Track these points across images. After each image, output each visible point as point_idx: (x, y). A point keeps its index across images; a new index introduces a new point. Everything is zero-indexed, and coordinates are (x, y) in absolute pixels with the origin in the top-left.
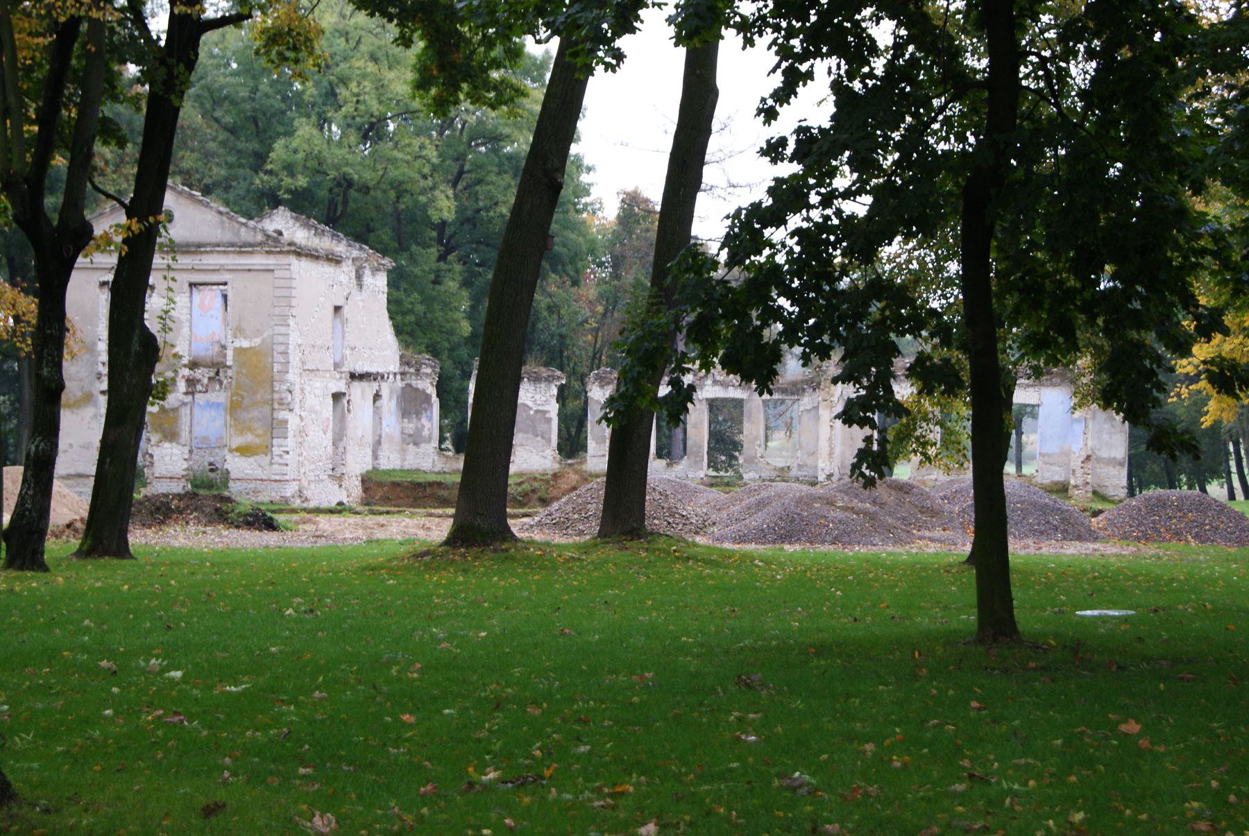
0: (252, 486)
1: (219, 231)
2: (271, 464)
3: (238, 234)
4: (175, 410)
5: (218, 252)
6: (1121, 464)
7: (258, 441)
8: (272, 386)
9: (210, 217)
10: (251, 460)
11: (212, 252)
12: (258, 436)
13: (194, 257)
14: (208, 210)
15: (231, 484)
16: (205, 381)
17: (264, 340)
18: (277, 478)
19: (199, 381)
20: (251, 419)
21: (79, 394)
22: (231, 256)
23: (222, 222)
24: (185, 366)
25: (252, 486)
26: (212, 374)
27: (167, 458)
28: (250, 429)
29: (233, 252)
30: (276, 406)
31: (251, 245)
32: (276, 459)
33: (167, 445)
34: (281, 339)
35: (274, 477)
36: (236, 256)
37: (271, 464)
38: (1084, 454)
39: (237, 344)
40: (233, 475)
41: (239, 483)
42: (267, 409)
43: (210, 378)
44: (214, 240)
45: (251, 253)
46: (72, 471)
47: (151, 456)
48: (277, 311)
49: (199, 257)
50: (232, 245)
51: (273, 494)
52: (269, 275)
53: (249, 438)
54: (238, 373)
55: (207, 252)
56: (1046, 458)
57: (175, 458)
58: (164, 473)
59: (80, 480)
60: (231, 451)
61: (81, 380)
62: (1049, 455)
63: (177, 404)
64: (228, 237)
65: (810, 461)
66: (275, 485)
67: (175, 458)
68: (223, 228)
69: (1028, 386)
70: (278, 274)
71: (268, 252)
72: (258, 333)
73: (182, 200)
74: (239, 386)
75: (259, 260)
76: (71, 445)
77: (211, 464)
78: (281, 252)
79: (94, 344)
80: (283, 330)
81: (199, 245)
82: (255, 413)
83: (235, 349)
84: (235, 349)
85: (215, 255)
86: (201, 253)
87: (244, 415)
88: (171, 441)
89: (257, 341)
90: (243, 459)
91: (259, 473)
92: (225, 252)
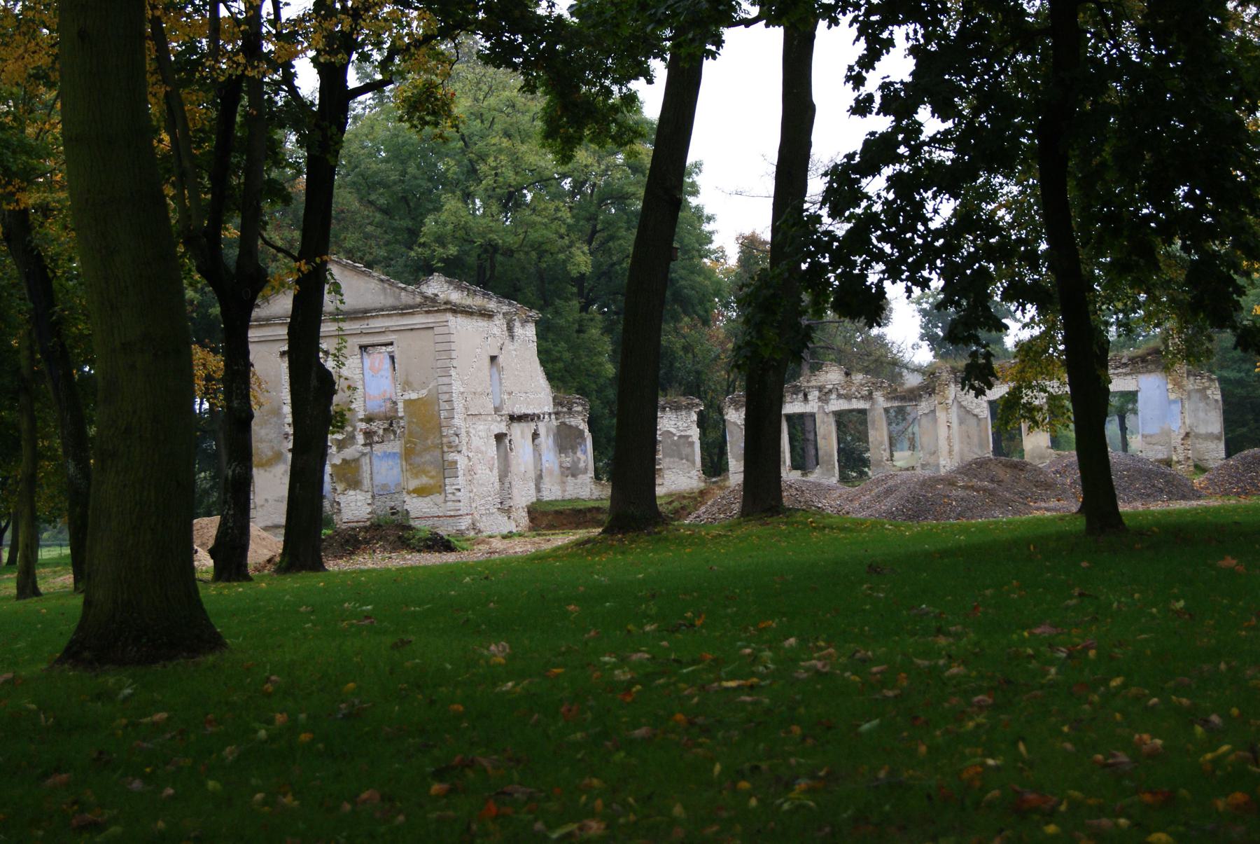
0: (430, 523)
2: (446, 501)
3: (399, 298)
4: (356, 460)
6: (1218, 438)
7: (432, 482)
8: (441, 432)
10: (428, 499)
11: (377, 316)
12: (432, 477)
16: (381, 432)
19: (375, 433)
20: (424, 463)
21: (270, 454)
23: (384, 289)
24: (361, 420)
25: (430, 523)
26: (386, 426)
28: (425, 473)
30: (446, 449)
31: (411, 307)
32: (450, 496)
33: (352, 492)
34: (445, 388)
38: (1183, 432)
39: (406, 397)
40: (412, 515)
42: (437, 453)
43: (384, 429)
44: (379, 306)
46: (269, 524)
47: (338, 503)
48: (439, 364)
50: (395, 308)
52: (430, 332)
53: (424, 480)
54: (409, 423)
56: (1149, 439)
60: (409, 493)
61: (271, 441)
62: (1151, 436)
63: (357, 455)
64: (390, 301)
65: (931, 460)
69: (1126, 374)
70: (437, 330)
71: (427, 312)
72: (424, 385)
73: (347, 273)
74: (411, 434)
75: (419, 320)
76: (266, 500)
77: (392, 508)
78: (437, 311)
79: (280, 408)
80: (446, 380)
81: (366, 311)
83: (406, 402)
84: (406, 402)
85: (380, 319)
86: (368, 318)
87: (418, 460)
89: (424, 393)
92: (388, 315)
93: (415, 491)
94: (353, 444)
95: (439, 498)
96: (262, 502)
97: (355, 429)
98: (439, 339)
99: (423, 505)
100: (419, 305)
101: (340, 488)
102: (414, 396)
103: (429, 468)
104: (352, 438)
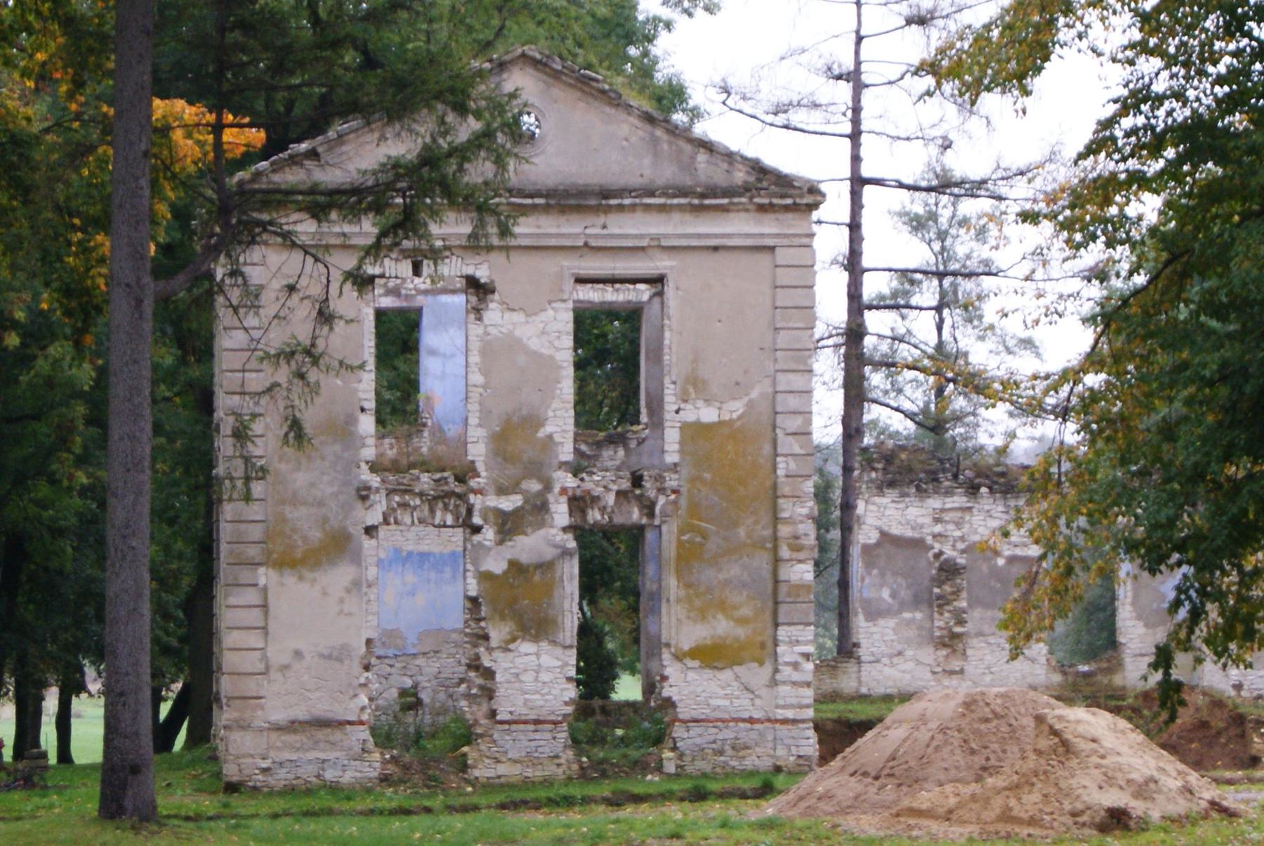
0: (728, 734)
1: (647, 161)
2: (774, 683)
3: (690, 167)
4: (546, 567)
5: (648, 207)
7: (741, 632)
8: (775, 509)
9: (625, 129)
10: (727, 675)
11: (633, 207)
12: (742, 621)
13: (590, 219)
14: (622, 115)
15: (678, 731)
16: (611, 499)
17: (750, 405)
18: (790, 714)
19: (595, 500)
20: (727, 582)
21: (316, 535)
22: (676, 216)
23: (655, 141)
24: (563, 465)
25: (728, 734)
27: (528, 677)
28: (723, 607)
29: (680, 207)
30: (785, 552)
31: (729, 192)
32: (786, 672)
33: (526, 647)
34: (793, 402)
35: (781, 714)
36: (688, 217)
37: (774, 683)
39: (689, 415)
40: (684, 712)
41: (695, 730)
42: (762, 561)
44: (635, 181)
45: (724, 209)
46: (301, 713)
47: (489, 674)
48: (783, 339)
49: (601, 219)
51: (781, 752)
52: (764, 259)
53: (722, 627)
54: (693, 480)
55: (621, 208)
57: (545, 677)
58: (522, 711)
59: (321, 734)
60: (679, 657)
61: (321, 503)
63: (549, 553)
64: (668, 173)
65: (956, 739)
66: (783, 730)
67: (545, 677)
68: (656, 154)
70: (782, 256)
71: (762, 208)
72: (738, 388)
73: (558, 92)
74: (694, 509)
75: (740, 226)
76: (298, 654)
78: (787, 208)
79: (351, 421)
80: (796, 381)
81: (606, 193)
82: (733, 570)
83: (685, 427)
84: (685, 427)
85: (639, 215)
86: (608, 209)
87: (708, 576)
88: (536, 639)
89: (735, 409)
90: (708, 673)
91: (744, 706)
92: (662, 208)
93: (695, 653)
94: (541, 524)
95: (757, 675)
96: (285, 659)
97: (548, 487)
98: (784, 277)
99: (713, 687)
100: (746, 189)
101: (498, 633)
102: (709, 415)
103: (735, 598)
104: (538, 509)
